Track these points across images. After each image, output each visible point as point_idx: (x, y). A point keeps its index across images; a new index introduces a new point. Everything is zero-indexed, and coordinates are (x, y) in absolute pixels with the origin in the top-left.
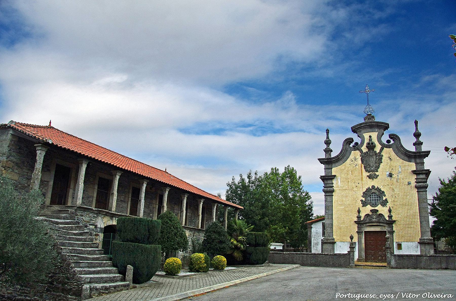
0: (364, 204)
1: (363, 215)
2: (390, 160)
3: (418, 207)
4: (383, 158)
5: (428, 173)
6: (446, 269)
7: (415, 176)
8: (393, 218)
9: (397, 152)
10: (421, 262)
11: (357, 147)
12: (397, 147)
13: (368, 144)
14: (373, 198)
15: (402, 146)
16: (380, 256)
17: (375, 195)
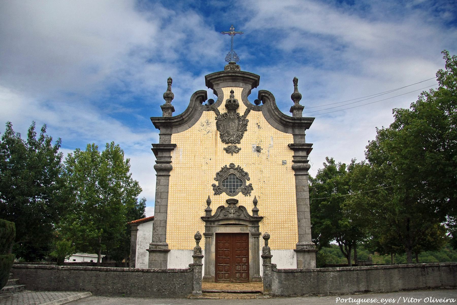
0: (217, 191)
1: (214, 208)
2: (259, 129)
3: (295, 198)
4: (249, 124)
5: (308, 149)
6: (367, 292)
7: (292, 153)
8: (259, 213)
9: (269, 117)
10: (325, 282)
11: (212, 106)
12: (269, 111)
13: (230, 101)
14: (230, 182)
15: (276, 109)
16: (239, 272)
17: (234, 179)
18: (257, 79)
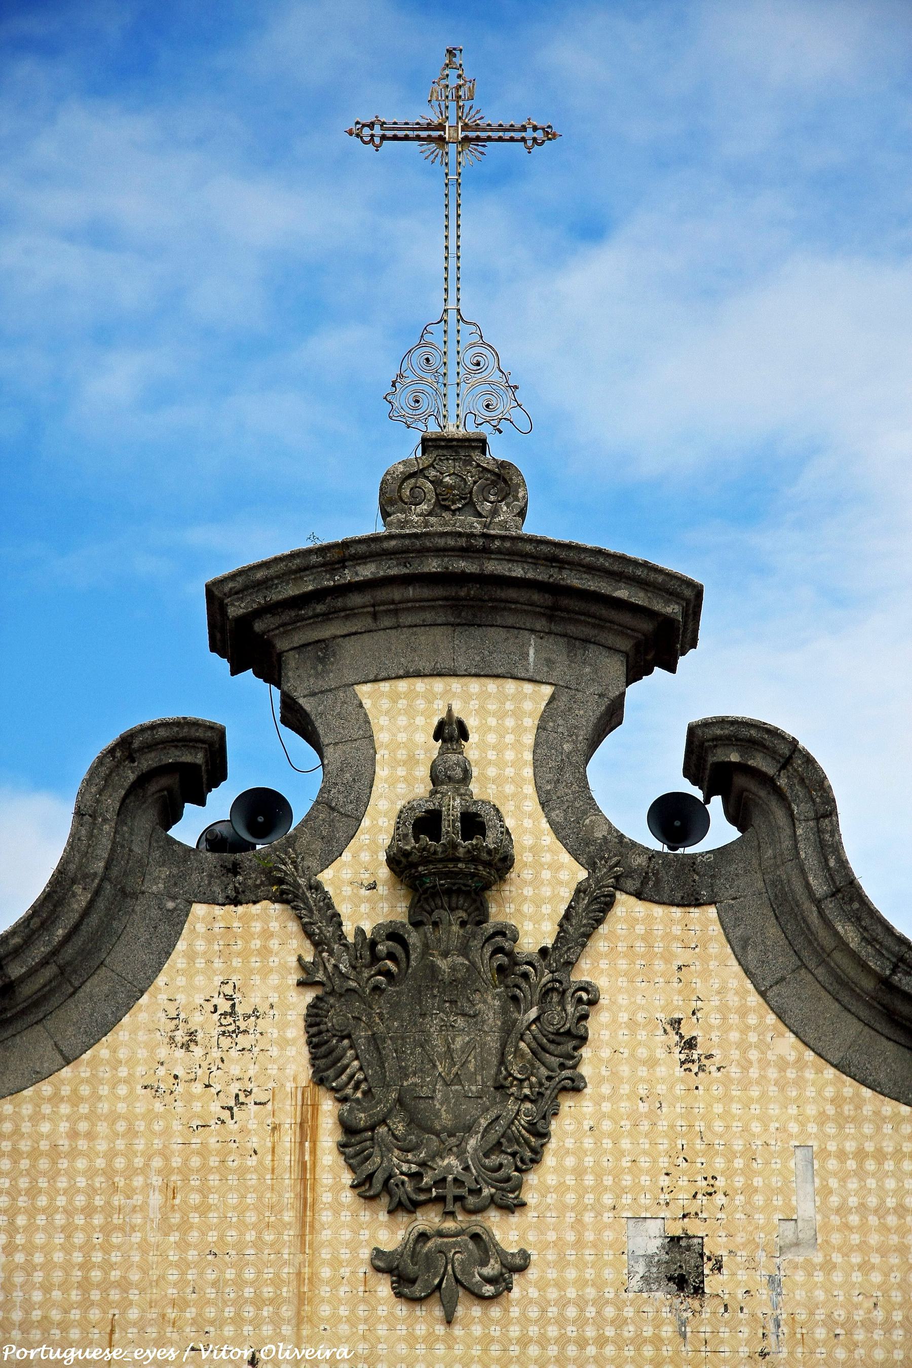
4: (599, 1025)
9: (783, 961)
11: (262, 852)
12: (782, 905)
13: (426, 822)
18: (672, 609)
